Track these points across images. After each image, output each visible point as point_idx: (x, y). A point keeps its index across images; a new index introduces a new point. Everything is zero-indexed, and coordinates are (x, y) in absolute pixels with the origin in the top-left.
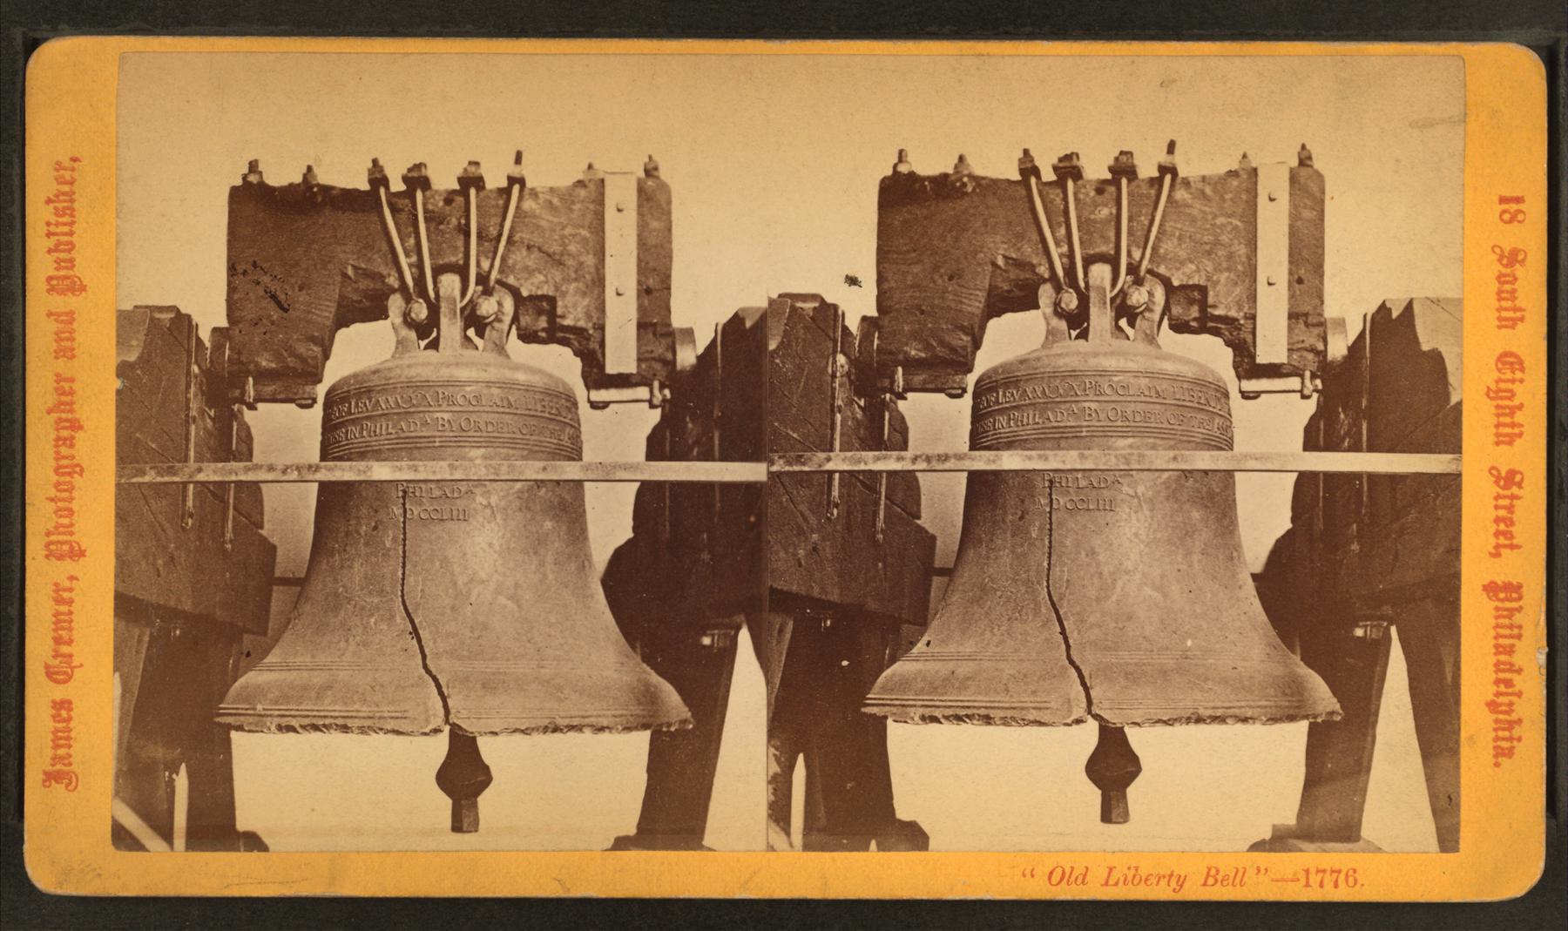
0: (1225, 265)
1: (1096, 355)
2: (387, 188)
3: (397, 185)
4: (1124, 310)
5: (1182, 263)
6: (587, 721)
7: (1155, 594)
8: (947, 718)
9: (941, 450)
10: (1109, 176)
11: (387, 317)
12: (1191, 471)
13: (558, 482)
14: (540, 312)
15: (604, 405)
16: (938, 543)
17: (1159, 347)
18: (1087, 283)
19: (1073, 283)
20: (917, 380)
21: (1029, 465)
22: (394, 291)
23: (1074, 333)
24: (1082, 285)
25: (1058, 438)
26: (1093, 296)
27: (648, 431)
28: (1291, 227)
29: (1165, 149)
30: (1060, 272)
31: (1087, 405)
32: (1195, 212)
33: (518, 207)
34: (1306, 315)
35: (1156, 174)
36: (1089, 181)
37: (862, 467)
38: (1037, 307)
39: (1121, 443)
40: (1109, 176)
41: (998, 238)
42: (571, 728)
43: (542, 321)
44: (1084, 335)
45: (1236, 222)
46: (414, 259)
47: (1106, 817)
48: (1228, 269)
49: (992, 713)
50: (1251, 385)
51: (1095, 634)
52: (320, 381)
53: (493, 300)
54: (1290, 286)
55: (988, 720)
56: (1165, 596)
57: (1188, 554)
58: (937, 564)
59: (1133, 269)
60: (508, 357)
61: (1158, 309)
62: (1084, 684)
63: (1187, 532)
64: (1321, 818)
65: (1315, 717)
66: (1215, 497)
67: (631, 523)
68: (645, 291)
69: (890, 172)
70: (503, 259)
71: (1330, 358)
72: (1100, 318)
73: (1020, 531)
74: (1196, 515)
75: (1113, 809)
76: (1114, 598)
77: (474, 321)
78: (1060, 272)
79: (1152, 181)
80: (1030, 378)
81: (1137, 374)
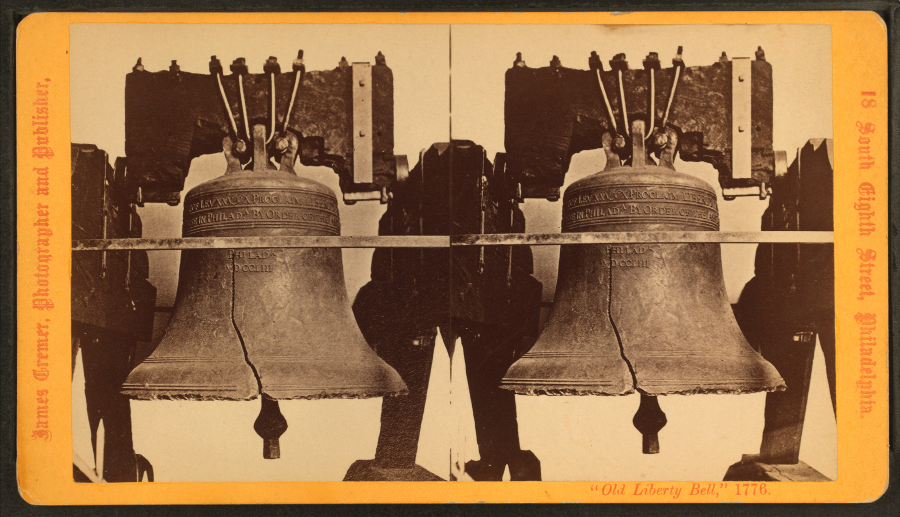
0: (713, 120)
1: (637, 174)
2: (221, 73)
3: (227, 72)
5: (688, 119)
6: (345, 391)
7: (674, 317)
8: (550, 391)
9: (546, 232)
10: (643, 68)
11: (221, 150)
12: (694, 244)
13: (326, 248)
14: (314, 147)
15: (353, 202)
16: (544, 289)
17: (674, 169)
21: (597, 241)
22: (226, 135)
23: (623, 162)
25: (614, 225)
26: (634, 139)
27: (380, 217)
28: (753, 96)
29: (676, 51)
31: (631, 204)
32: (695, 88)
33: (300, 84)
34: (762, 148)
35: (672, 66)
36: (631, 71)
37: (498, 243)
38: (601, 146)
39: (652, 227)
40: (643, 68)
42: (335, 395)
43: (314, 152)
44: (629, 163)
45: (719, 94)
46: (238, 115)
47: (646, 450)
48: (715, 123)
49: (577, 389)
50: (730, 192)
51: (635, 342)
52: (182, 189)
53: (286, 140)
54: (753, 132)
55: (574, 392)
56: (680, 317)
57: (693, 293)
58: (544, 300)
60: (295, 174)
61: (673, 147)
62: (631, 370)
63: (692, 280)
64: (773, 451)
65: (770, 389)
66: (708, 259)
67: (369, 273)
68: (377, 134)
69: (511, 66)
71: (777, 173)
72: (639, 154)
73: (593, 280)
74: (697, 269)
75: (650, 445)
76: (649, 319)
77: (273, 151)
79: (668, 70)
80: (597, 189)
81: (661, 186)
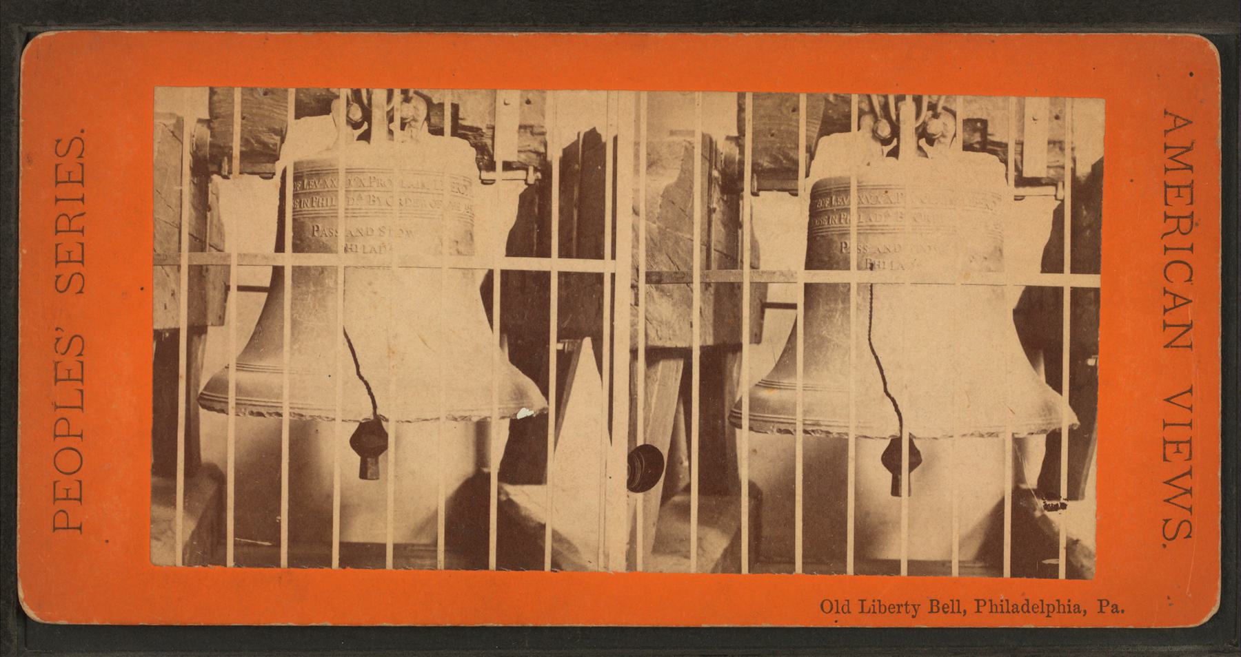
19: (887, 115)
20: (767, 184)
26: (903, 127)
30: (878, 109)
59: (932, 107)
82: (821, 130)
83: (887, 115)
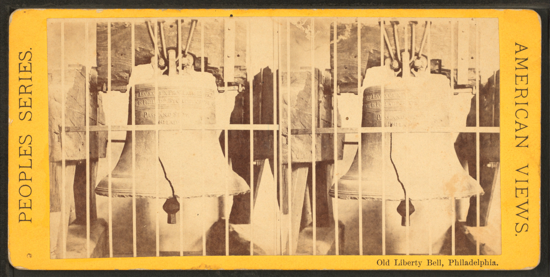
4: (413, 67)
18: (401, 59)
19: (397, 59)
20: (343, 90)
24: (400, 59)
30: (392, 56)
41: (371, 44)
59: (417, 54)
70: (190, 46)
78: (392, 56)
82: (368, 65)
83: (397, 59)
